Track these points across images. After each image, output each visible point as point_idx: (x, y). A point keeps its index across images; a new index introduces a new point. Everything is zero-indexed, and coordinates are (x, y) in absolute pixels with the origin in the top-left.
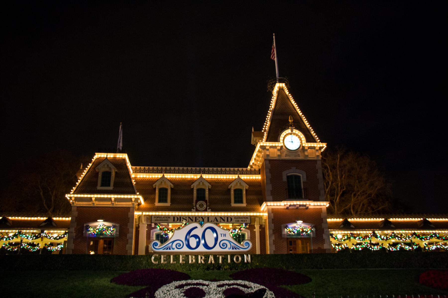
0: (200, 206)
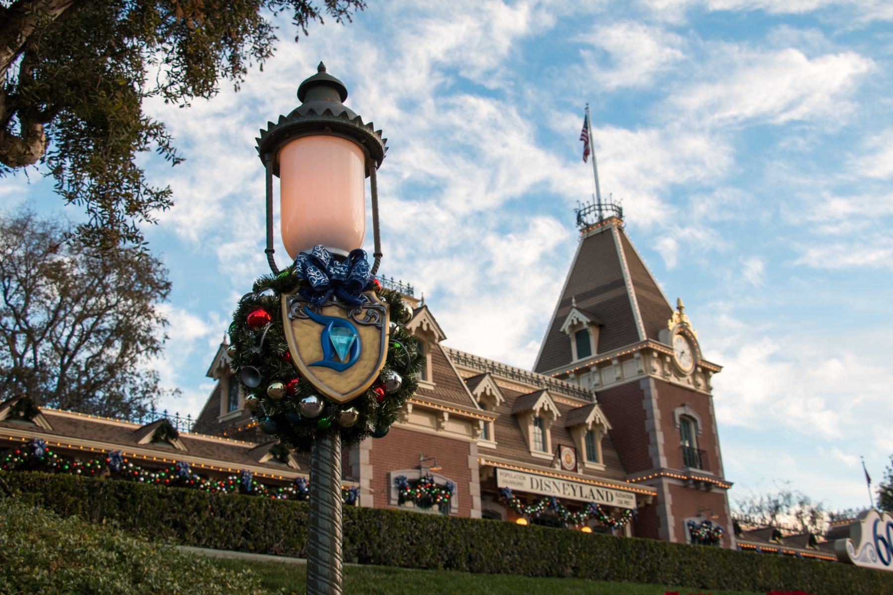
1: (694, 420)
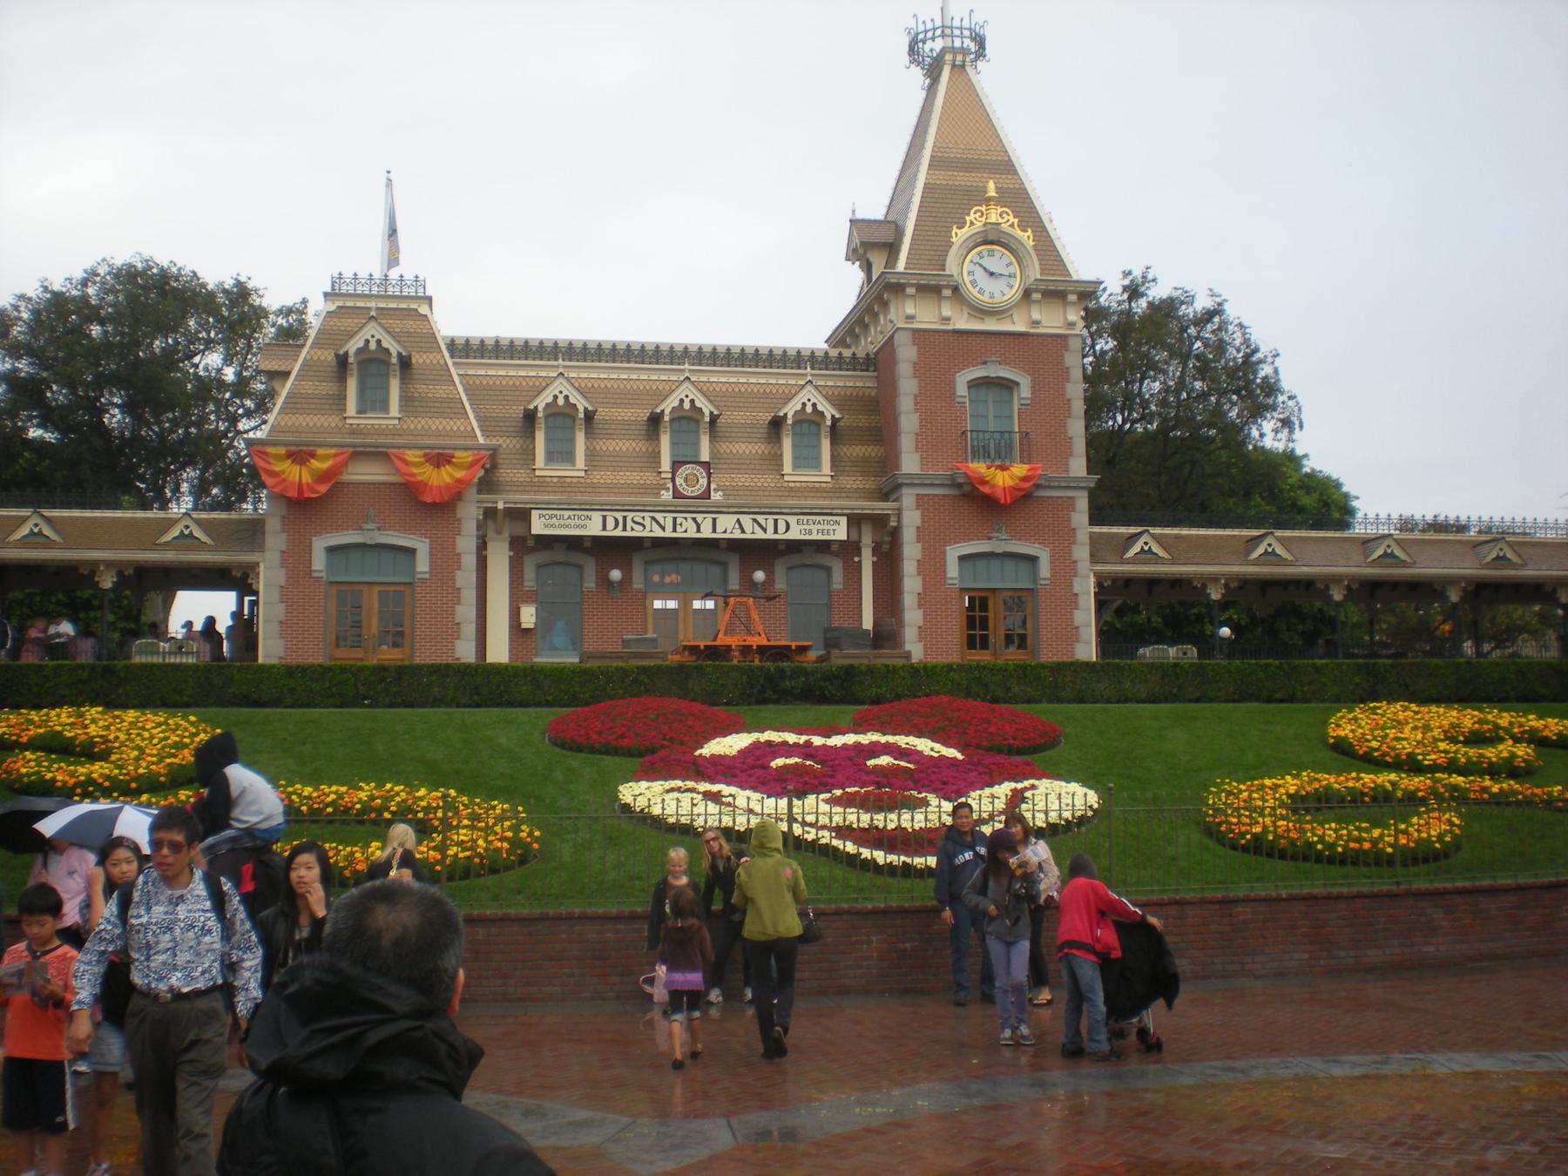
0: (686, 480)
1: (1017, 384)
